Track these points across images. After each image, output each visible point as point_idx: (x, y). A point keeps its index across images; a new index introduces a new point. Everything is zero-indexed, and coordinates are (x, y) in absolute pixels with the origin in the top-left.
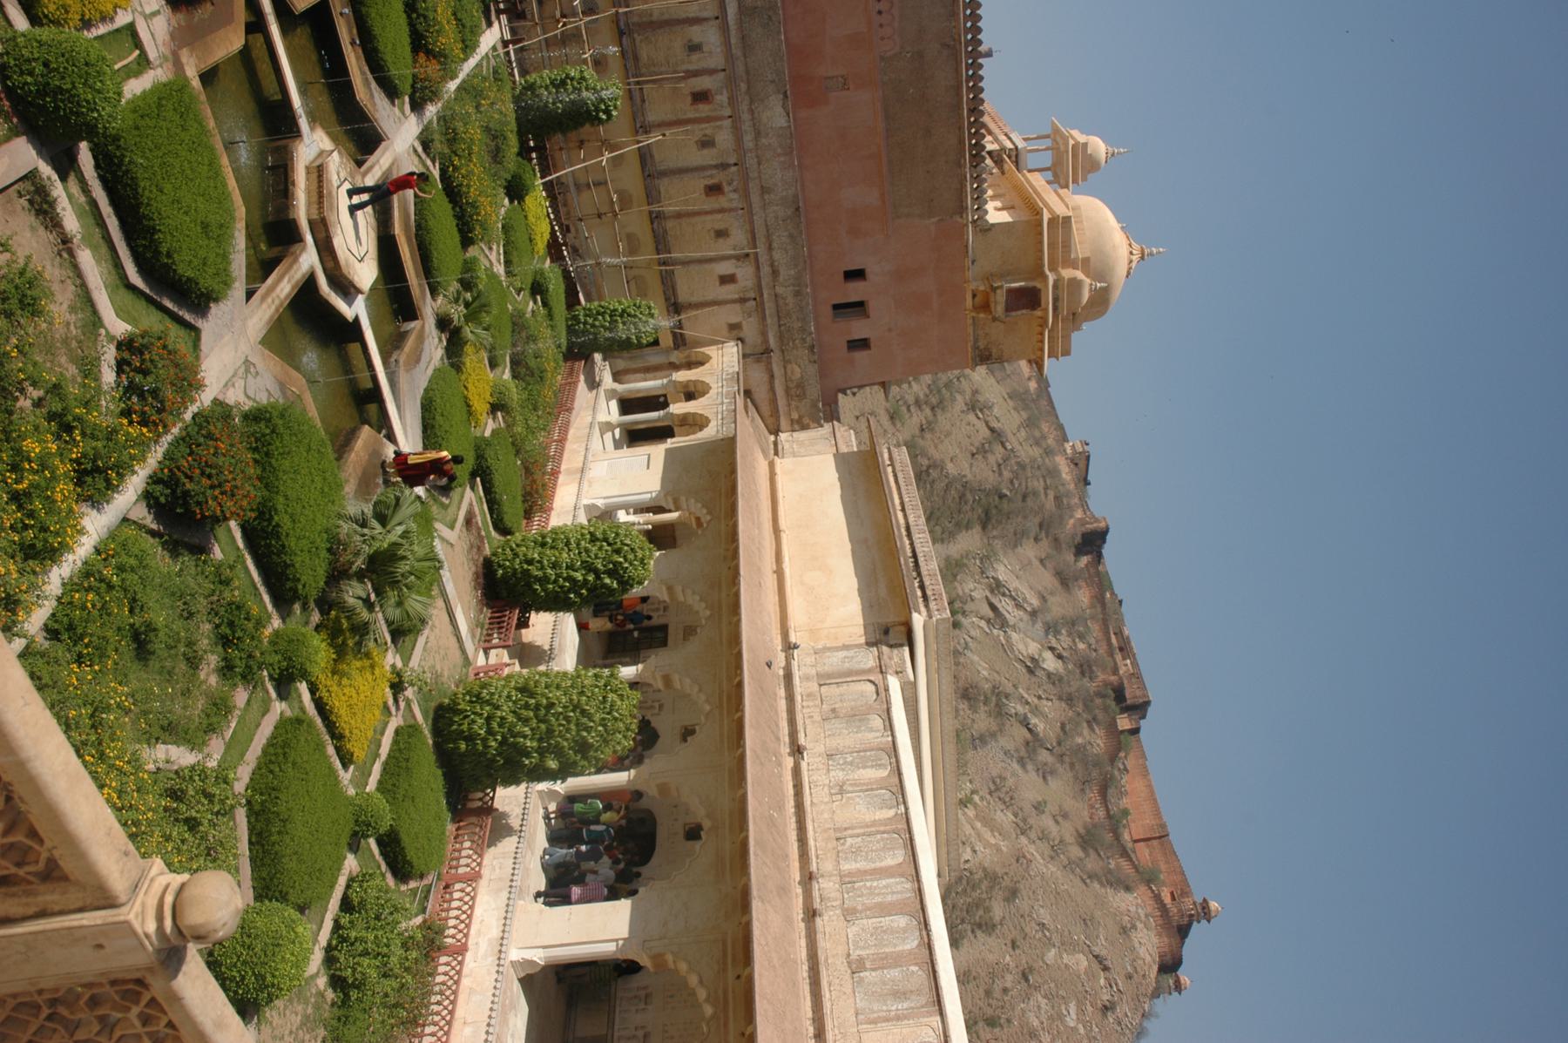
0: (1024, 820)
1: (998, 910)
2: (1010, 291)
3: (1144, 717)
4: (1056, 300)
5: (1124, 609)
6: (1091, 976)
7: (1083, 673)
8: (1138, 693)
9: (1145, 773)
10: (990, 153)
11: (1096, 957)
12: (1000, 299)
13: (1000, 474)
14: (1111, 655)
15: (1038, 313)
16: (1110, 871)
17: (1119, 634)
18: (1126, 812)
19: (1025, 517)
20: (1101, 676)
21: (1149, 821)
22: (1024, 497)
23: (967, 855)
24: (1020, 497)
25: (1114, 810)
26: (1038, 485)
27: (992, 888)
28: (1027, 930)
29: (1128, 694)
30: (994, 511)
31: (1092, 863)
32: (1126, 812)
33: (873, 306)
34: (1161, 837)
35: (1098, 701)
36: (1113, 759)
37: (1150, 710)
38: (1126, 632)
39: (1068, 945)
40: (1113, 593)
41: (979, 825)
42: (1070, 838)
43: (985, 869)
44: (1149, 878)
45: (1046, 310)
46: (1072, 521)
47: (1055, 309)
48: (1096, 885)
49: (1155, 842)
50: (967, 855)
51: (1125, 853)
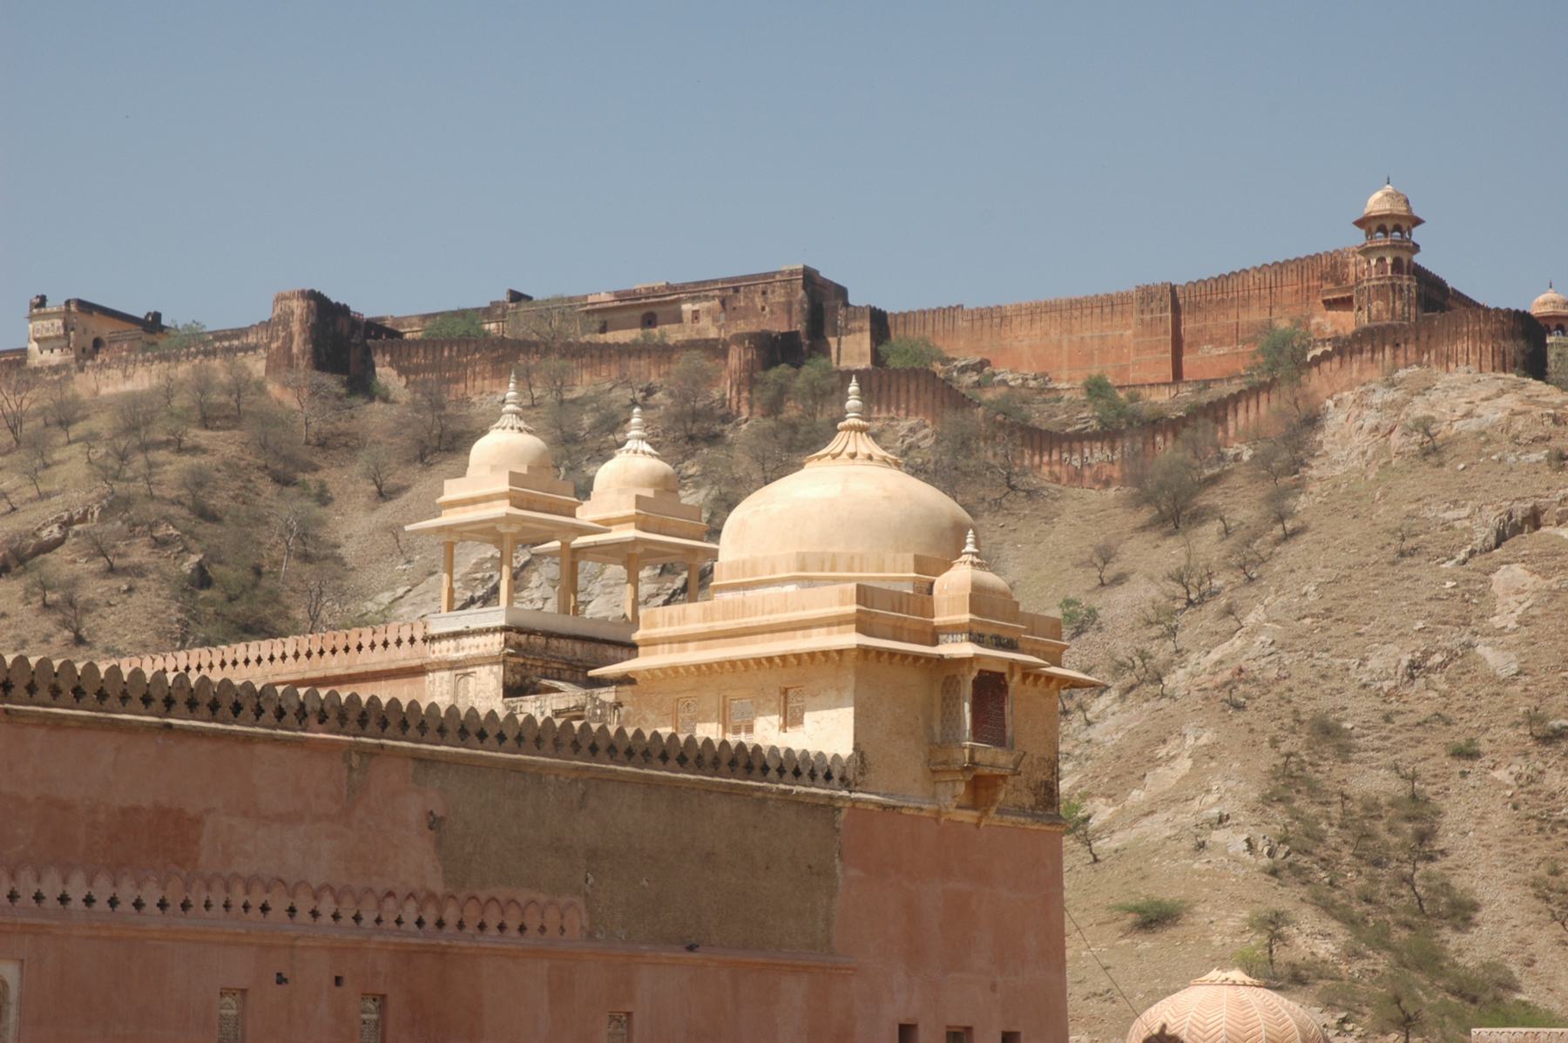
0: (1119, 668)
1: (1372, 780)
2: (976, 735)
3: (842, 292)
4: (999, 643)
5: (538, 295)
6: (1548, 561)
7: (714, 439)
8: (778, 297)
9: (994, 317)
10: (510, 690)
11: (1501, 539)
12: (992, 757)
13: (139, 571)
14: (665, 352)
15: (1014, 682)
16: (1262, 461)
17: (605, 317)
18: (1096, 388)
19: (261, 521)
20: (724, 389)
21: (1126, 331)
22: (208, 515)
23: (1232, 840)
24: (205, 529)
25: (1088, 418)
26: (174, 467)
27: (1313, 790)
28: (1425, 710)
29: (778, 326)
30: (240, 608)
31: (1241, 504)
32: (1096, 388)
33: (956, 1019)
34: (1175, 308)
35: (792, 411)
36: (961, 401)
37: (829, 272)
38: (604, 297)
39: (1470, 606)
40: (488, 313)
41: (1137, 796)
42: (1171, 553)
43: (1268, 800)
44: (1287, 361)
45: (1012, 664)
46: (274, 389)
47: (1011, 646)
48: (1302, 503)
49: (1188, 325)
50: (1232, 840)
51: (1217, 411)
